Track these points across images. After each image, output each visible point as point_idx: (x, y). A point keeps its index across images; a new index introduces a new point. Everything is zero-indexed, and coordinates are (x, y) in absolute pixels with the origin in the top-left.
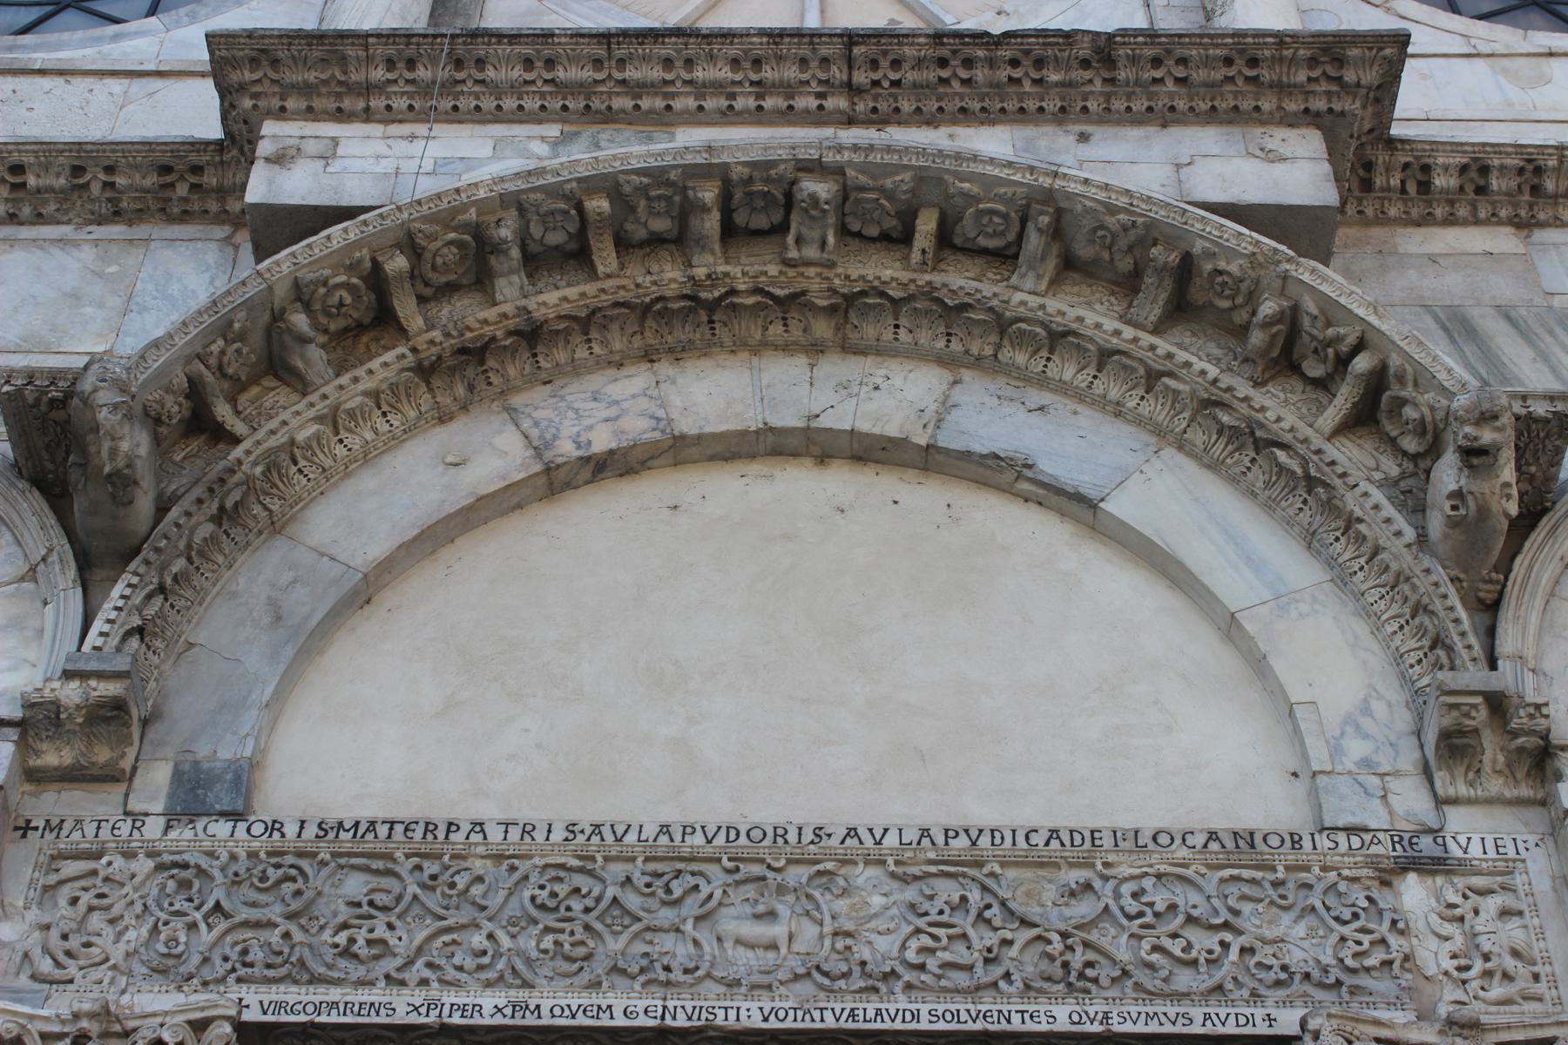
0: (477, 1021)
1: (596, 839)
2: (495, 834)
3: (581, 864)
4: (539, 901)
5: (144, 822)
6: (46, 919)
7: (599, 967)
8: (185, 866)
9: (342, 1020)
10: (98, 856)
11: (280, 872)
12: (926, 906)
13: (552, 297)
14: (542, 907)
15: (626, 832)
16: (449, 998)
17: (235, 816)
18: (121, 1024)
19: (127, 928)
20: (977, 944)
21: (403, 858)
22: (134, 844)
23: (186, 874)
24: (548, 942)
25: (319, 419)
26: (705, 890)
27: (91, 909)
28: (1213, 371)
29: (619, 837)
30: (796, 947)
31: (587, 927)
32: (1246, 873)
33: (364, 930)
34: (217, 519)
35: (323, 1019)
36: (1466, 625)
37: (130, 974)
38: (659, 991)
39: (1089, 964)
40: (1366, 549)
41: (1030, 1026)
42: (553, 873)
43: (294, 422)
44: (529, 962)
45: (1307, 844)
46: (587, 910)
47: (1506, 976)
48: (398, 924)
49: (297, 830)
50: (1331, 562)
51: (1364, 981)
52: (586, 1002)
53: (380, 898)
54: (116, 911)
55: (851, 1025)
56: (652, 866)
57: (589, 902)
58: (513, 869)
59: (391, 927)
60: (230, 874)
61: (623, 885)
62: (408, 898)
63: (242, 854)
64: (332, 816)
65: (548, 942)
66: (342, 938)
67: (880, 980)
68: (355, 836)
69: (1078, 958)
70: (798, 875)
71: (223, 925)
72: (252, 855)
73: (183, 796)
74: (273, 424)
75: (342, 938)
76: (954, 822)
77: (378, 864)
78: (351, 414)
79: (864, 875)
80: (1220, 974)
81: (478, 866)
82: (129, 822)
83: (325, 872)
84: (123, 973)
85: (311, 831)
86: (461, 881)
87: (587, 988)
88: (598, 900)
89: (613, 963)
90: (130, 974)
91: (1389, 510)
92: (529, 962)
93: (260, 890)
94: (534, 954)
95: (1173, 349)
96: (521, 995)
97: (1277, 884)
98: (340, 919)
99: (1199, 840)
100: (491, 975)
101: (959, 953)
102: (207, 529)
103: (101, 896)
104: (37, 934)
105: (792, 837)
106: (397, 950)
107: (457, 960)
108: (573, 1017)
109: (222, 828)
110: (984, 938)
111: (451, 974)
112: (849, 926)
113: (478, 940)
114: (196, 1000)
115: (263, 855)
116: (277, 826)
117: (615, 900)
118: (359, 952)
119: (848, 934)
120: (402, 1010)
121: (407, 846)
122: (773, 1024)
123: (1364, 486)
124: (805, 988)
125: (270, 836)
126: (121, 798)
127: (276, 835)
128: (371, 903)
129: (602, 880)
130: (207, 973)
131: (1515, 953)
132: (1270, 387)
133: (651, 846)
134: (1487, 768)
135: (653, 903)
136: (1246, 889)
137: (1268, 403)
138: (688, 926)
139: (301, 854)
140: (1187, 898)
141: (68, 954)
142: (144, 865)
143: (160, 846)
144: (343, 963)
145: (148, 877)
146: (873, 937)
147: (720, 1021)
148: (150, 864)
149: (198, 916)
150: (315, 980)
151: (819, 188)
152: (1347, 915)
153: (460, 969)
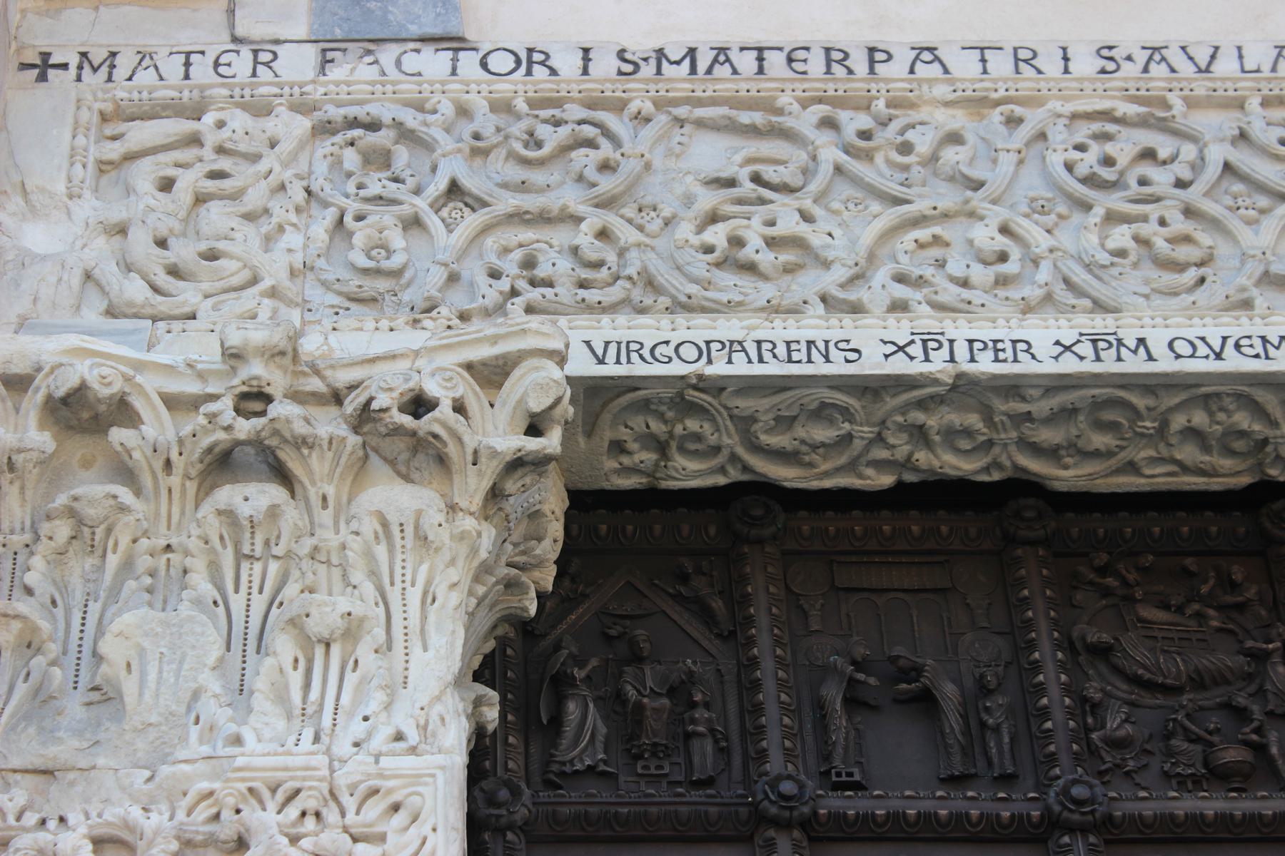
0: (1026, 366)
1: (1158, 70)
3: (1142, 109)
4: (1082, 170)
5: (275, 55)
6: (117, 214)
9: (758, 370)
11: (564, 131)
14: (1091, 180)
15: (1213, 57)
16: (959, 330)
17: (454, 43)
18: (323, 378)
19: (281, 229)
21: (796, 106)
22: (263, 90)
27: (201, 199)
29: (1203, 66)
33: (756, 222)
35: (719, 368)
37: (305, 306)
48: (817, 211)
49: (580, 63)
52: (1235, 332)
54: (255, 198)
58: (1013, 122)
59: (807, 217)
60: (467, 136)
61: (1234, 142)
62: (825, 170)
63: (480, 104)
64: (640, 45)
65: (1121, 236)
66: (717, 235)
68: (693, 70)
71: (472, 221)
72: (502, 107)
73: (341, 13)
75: (717, 235)
82: (246, 53)
83: (648, 132)
84: (291, 303)
85: (605, 65)
86: (923, 141)
87: (1227, 310)
89: (1261, 269)
90: (305, 306)
93: (526, 162)
94: (1104, 258)
96: (1101, 324)
100: (1032, 292)
106: (831, 255)
108: (1218, 356)
109: (434, 63)
111: (951, 293)
113: (985, 235)
115: (521, 105)
116: (537, 57)
117: (1227, 167)
118: (757, 258)
121: (797, 85)
125: (529, 73)
126: (221, 17)
127: (540, 72)
128: (757, 179)
130: (459, 299)
133: (1269, 80)
139: (591, 105)
141: (174, 272)
142: (296, 126)
143: (317, 93)
144: (727, 278)
145: (301, 146)
148: (303, 124)
150: (686, 307)
153: (965, 283)
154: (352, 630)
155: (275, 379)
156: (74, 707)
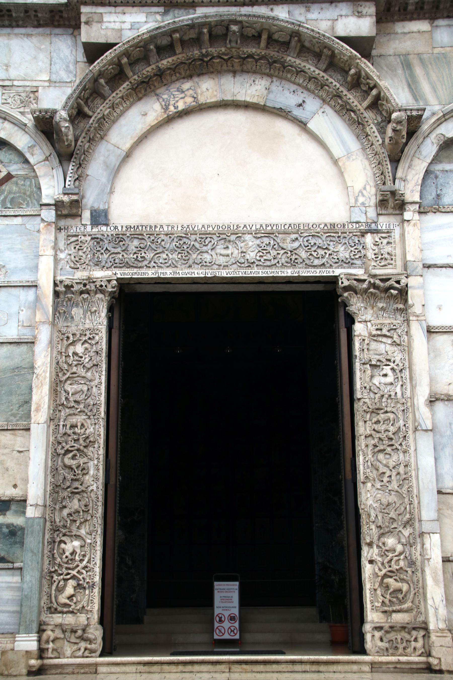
0: (166, 276)
2: (165, 229)
7: (191, 262)
8: (98, 238)
10: (78, 236)
12: (261, 245)
13: (165, 62)
14: (178, 247)
16: (160, 271)
17: (107, 225)
20: (272, 255)
23: (98, 240)
24: (180, 256)
25: (109, 108)
26: (213, 242)
28: (338, 85)
30: (233, 256)
31: (188, 252)
32: (332, 234)
34: (89, 142)
35: (134, 277)
36: (390, 170)
38: (205, 268)
39: (296, 259)
40: (370, 143)
41: (283, 275)
42: (179, 238)
43: (104, 109)
44: (176, 261)
45: (346, 227)
46: (187, 248)
47: (386, 259)
48: (146, 252)
50: (362, 144)
51: (355, 261)
53: (142, 246)
55: (245, 275)
56: (201, 236)
57: (188, 246)
58: (170, 237)
59: (145, 253)
62: (148, 246)
66: (135, 256)
67: (251, 264)
69: (293, 257)
70: (233, 237)
72: (112, 235)
74: (99, 111)
75: (135, 256)
76: (268, 223)
77: (140, 237)
78: (117, 104)
79: (248, 237)
80: (324, 260)
81: (163, 237)
83: (129, 239)
85: (124, 229)
86: (159, 241)
88: (190, 245)
91: (377, 134)
92: (176, 261)
94: (177, 259)
95: (329, 78)
97: (339, 237)
98: (134, 251)
99: (322, 226)
100: (168, 265)
101: (268, 257)
102: (88, 144)
103: (81, 246)
104: (68, 257)
105: (232, 228)
107: (161, 261)
109: (104, 228)
110: (274, 253)
111: (160, 265)
112: (245, 251)
113: (164, 256)
114: (108, 273)
119: (244, 252)
120: (150, 274)
122: (229, 275)
123: (372, 125)
124: (235, 266)
129: (190, 240)
130: (107, 265)
131: (388, 253)
132: (352, 91)
134: (389, 207)
135: (202, 246)
136: (332, 239)
137: (351, 97)
138: (210, 251)
139: (123, 235)
140: (319, 242)
142: (89, 238)
144: (136, 262)
146: (250, 253)
147: (217, 275)
148: (90, 238)
149: (103, 251)
151: (234, 28)
152: (353, 245)
153: (161, 263)
154: (95, 311)
155: (87, 282)
156: (69, 319)
